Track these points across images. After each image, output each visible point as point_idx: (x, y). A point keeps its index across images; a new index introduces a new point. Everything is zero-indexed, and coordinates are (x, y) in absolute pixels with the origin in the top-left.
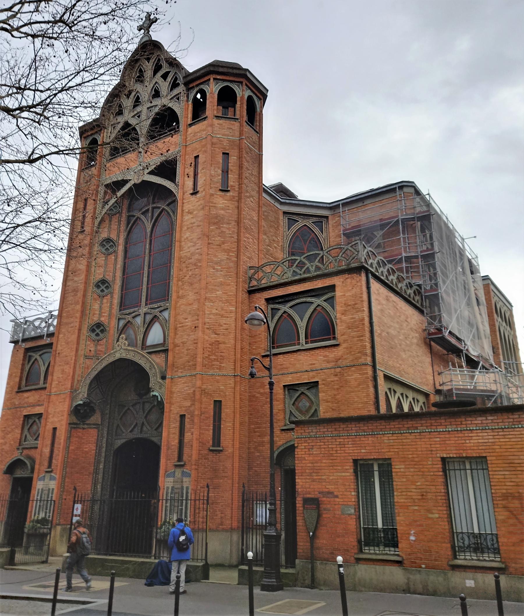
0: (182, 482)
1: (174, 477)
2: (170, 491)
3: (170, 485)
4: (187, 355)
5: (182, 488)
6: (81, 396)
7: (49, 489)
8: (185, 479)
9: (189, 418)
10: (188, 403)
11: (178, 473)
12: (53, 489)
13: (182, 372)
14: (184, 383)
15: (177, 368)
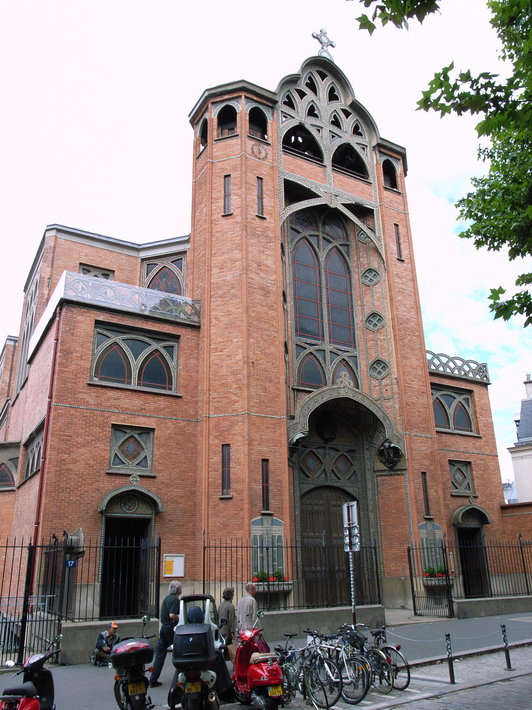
0: (434, 534)
1: (426, 529)
2: (425, 542)
3: (424, 536)
4: (419, 416)
5: (435, 538)
6: (300, 427)
7: (273, 537)
8: (436, 532)
9: (430, 476)
10: (427, 463)
11: (429, 524)
12: (280, 537)
13: (417, 432)
14: (420, 442)
15: (412, 426)
